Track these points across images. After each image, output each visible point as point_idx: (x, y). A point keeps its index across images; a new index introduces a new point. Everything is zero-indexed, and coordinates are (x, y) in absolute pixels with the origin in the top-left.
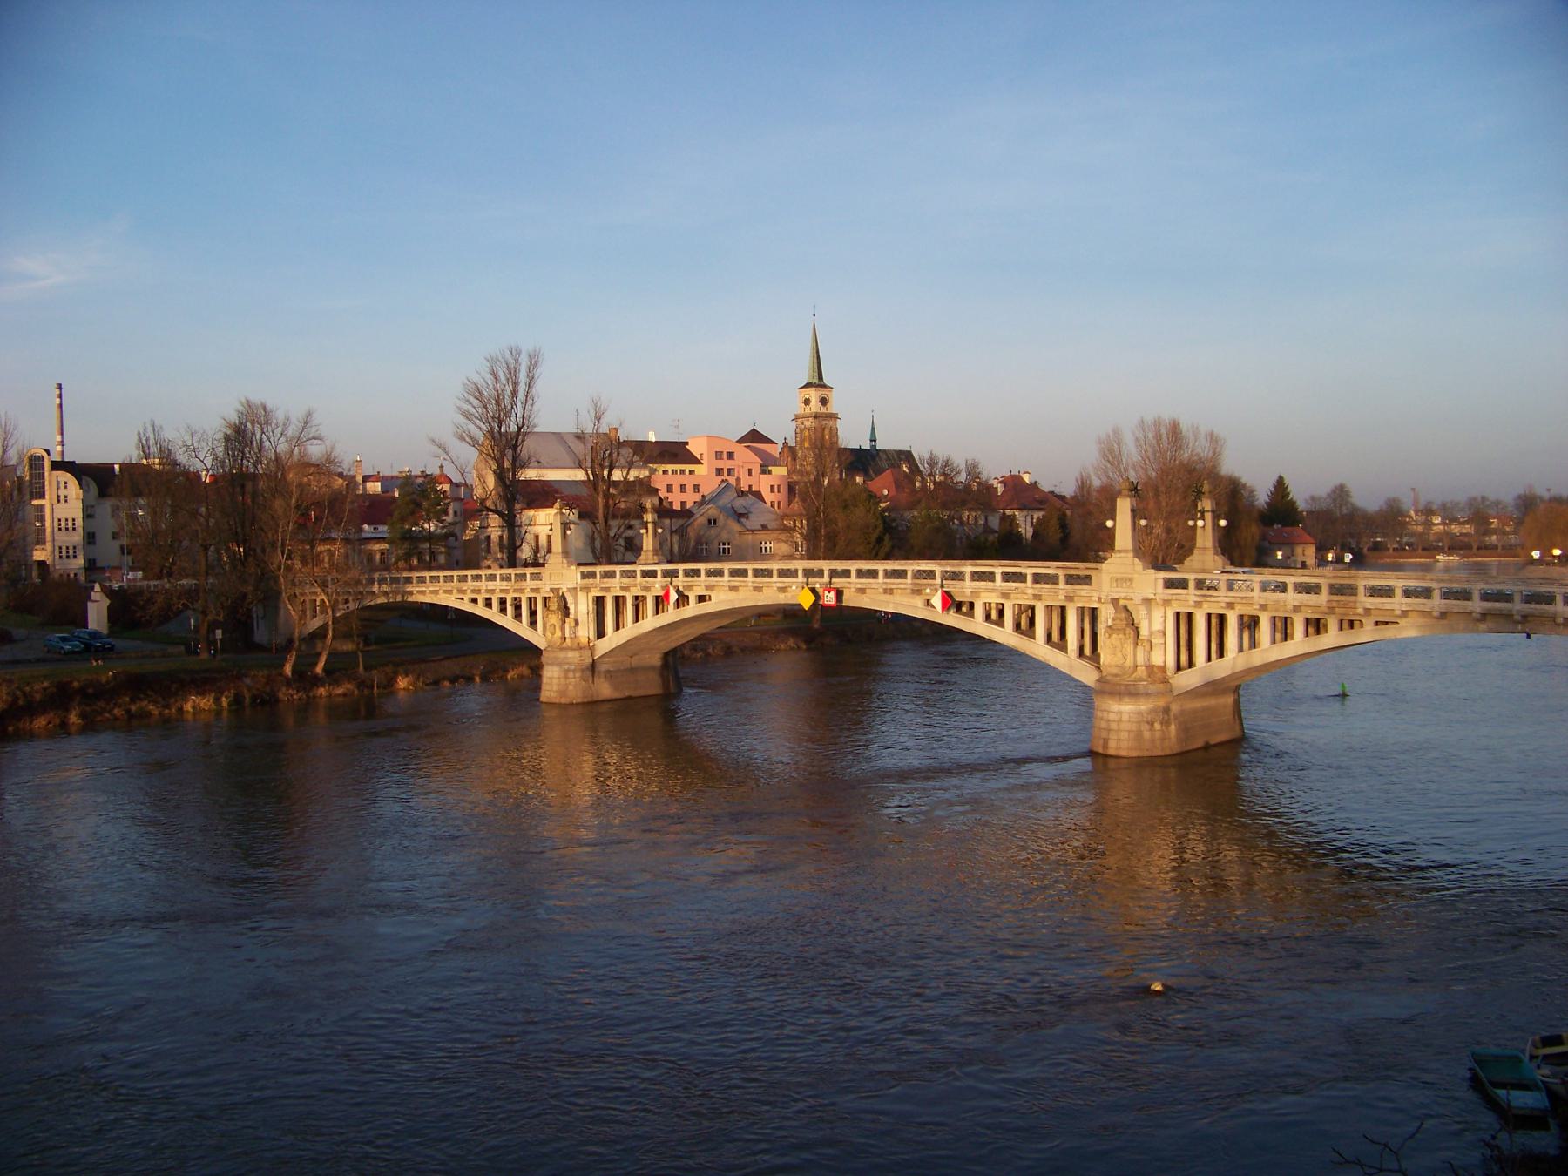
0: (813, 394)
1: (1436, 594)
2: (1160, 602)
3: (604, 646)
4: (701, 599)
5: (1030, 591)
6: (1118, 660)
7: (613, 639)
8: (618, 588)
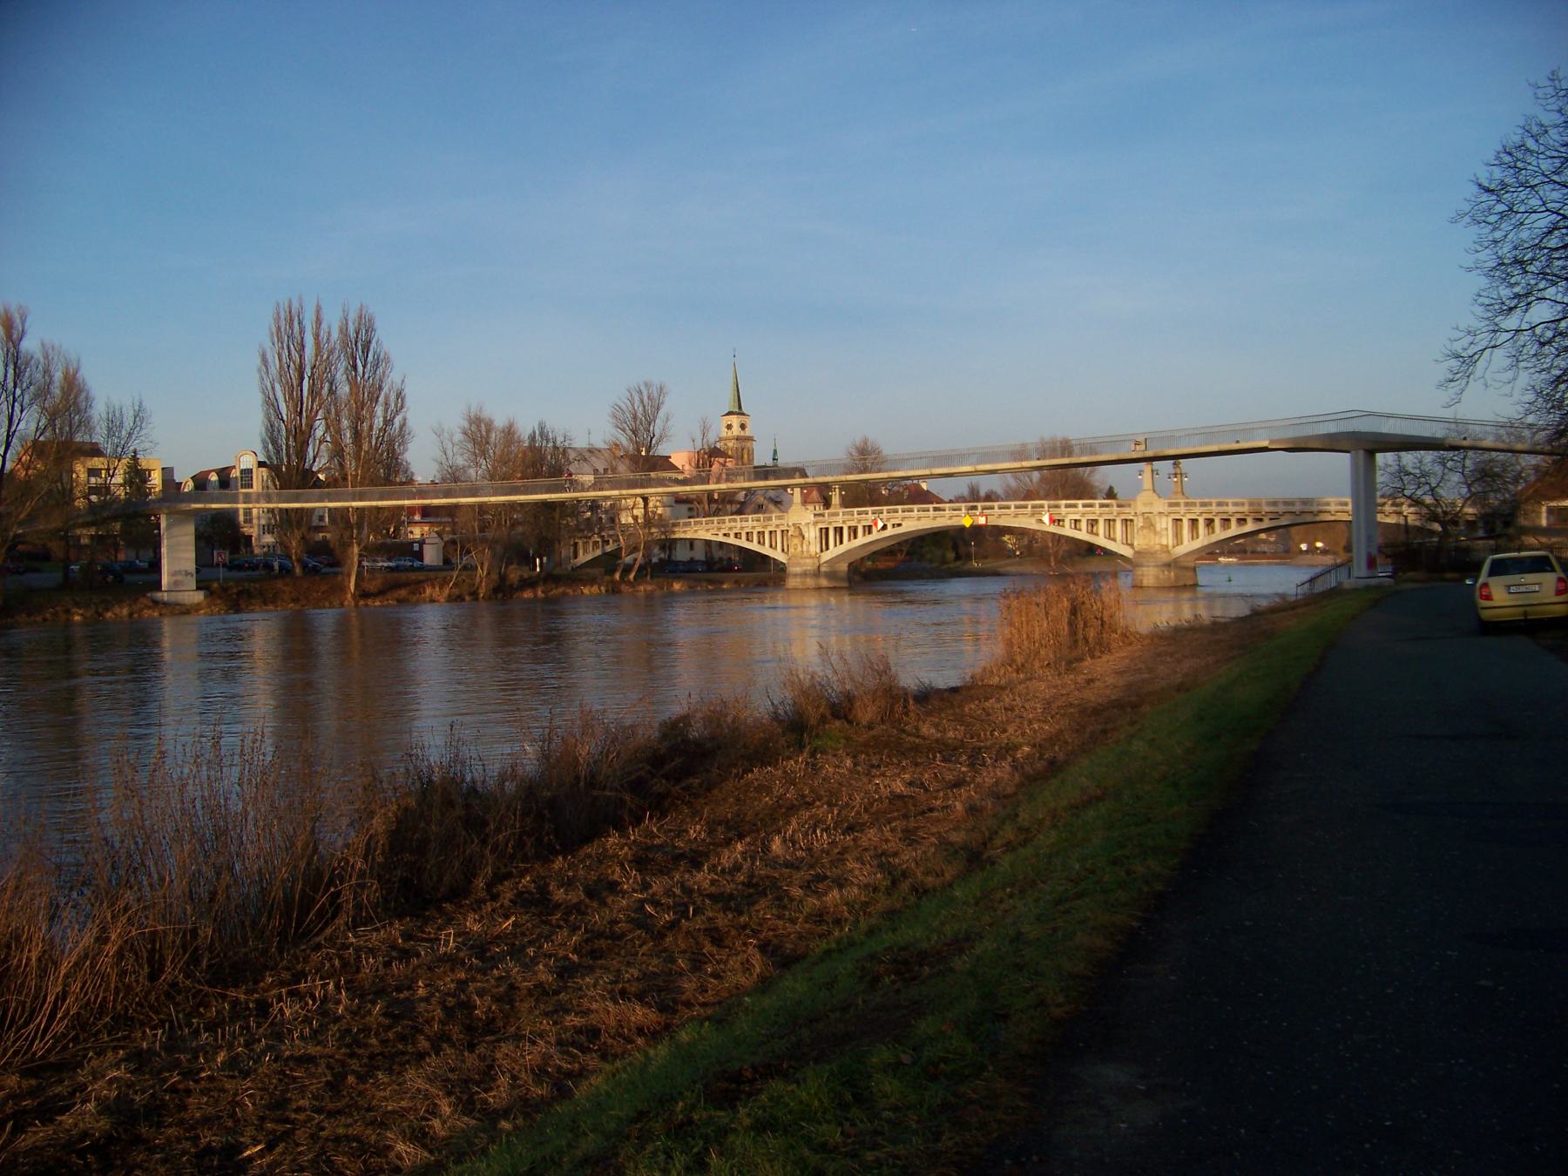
0: (735, 421)
3: (827, 556)
7: (834, 551)
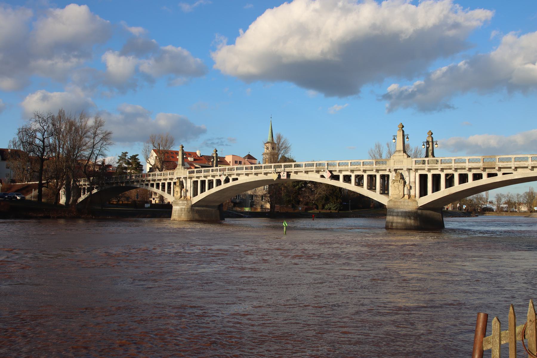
1: (530, 159)
2: (414, 170)
3: (195, 200)
4: (234, 180)
5: (362, 169)
6: (397, 192)
8: (203, 176)
